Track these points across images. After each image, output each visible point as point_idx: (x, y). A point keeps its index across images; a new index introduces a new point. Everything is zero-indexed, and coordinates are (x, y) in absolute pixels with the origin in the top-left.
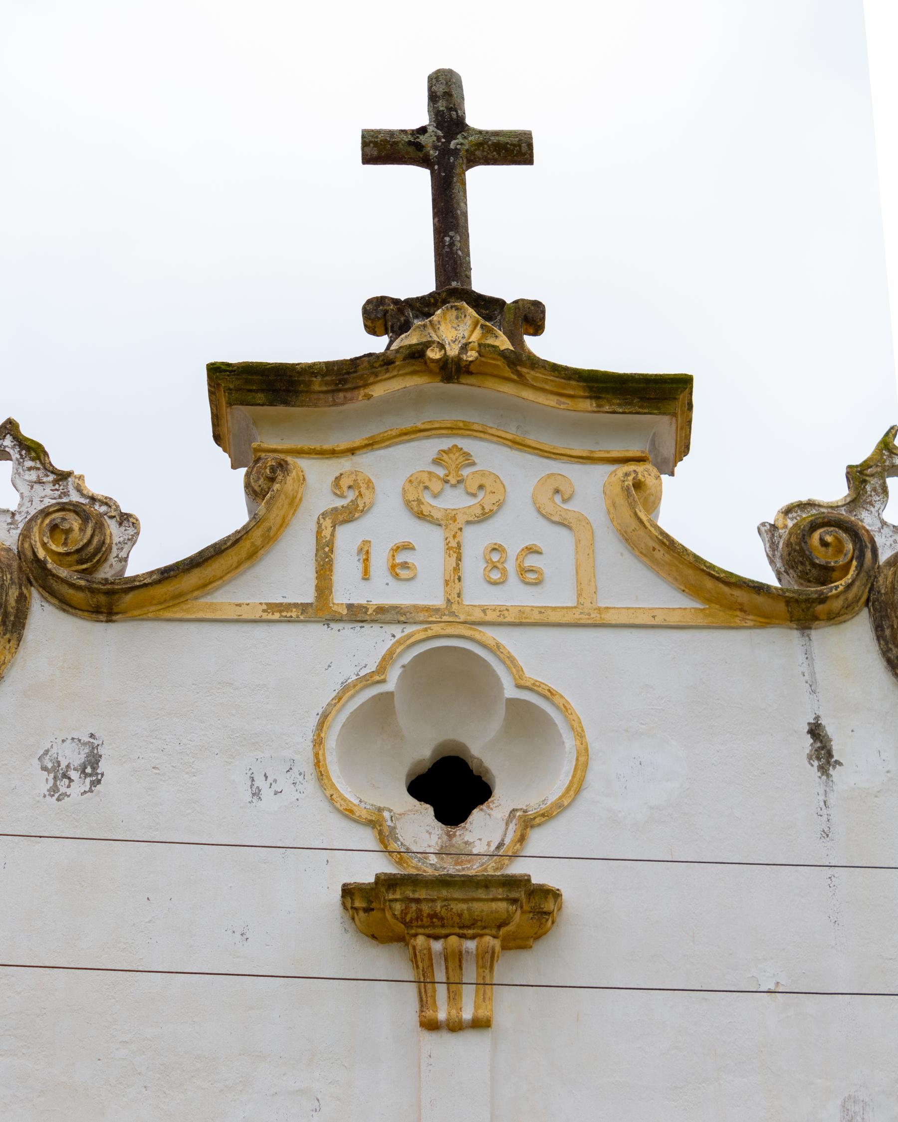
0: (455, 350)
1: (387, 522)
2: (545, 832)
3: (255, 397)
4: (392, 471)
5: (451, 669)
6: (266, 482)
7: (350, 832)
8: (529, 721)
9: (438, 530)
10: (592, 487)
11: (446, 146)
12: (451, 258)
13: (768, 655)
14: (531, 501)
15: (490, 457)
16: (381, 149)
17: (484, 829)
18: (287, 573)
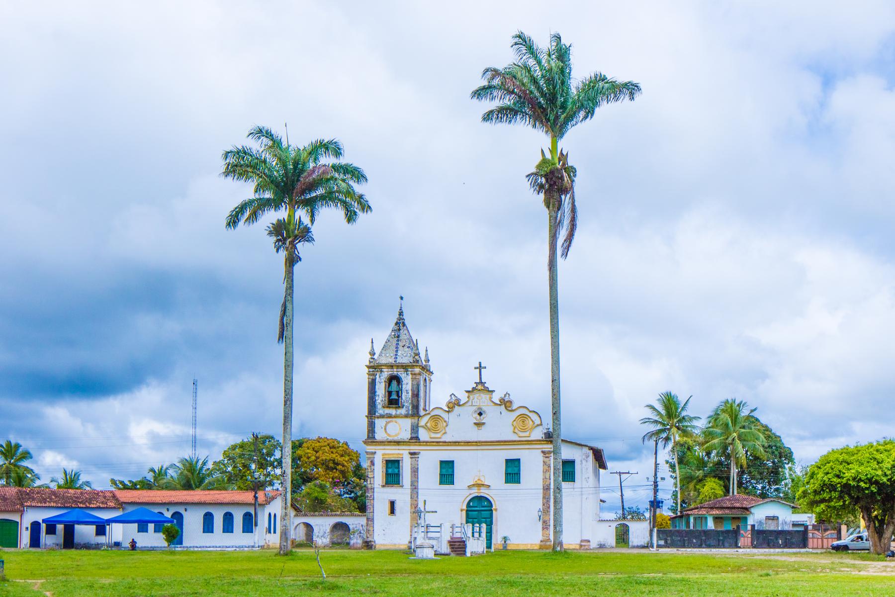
0: (480, 387)
1: (476, 400)
3: (468, 392)
4: (476, 396)
5: (480, 408)
10: (488, 396)
11: (480, 367)
14: (485, 397)
16: (476, 368)
18: (470, 403)
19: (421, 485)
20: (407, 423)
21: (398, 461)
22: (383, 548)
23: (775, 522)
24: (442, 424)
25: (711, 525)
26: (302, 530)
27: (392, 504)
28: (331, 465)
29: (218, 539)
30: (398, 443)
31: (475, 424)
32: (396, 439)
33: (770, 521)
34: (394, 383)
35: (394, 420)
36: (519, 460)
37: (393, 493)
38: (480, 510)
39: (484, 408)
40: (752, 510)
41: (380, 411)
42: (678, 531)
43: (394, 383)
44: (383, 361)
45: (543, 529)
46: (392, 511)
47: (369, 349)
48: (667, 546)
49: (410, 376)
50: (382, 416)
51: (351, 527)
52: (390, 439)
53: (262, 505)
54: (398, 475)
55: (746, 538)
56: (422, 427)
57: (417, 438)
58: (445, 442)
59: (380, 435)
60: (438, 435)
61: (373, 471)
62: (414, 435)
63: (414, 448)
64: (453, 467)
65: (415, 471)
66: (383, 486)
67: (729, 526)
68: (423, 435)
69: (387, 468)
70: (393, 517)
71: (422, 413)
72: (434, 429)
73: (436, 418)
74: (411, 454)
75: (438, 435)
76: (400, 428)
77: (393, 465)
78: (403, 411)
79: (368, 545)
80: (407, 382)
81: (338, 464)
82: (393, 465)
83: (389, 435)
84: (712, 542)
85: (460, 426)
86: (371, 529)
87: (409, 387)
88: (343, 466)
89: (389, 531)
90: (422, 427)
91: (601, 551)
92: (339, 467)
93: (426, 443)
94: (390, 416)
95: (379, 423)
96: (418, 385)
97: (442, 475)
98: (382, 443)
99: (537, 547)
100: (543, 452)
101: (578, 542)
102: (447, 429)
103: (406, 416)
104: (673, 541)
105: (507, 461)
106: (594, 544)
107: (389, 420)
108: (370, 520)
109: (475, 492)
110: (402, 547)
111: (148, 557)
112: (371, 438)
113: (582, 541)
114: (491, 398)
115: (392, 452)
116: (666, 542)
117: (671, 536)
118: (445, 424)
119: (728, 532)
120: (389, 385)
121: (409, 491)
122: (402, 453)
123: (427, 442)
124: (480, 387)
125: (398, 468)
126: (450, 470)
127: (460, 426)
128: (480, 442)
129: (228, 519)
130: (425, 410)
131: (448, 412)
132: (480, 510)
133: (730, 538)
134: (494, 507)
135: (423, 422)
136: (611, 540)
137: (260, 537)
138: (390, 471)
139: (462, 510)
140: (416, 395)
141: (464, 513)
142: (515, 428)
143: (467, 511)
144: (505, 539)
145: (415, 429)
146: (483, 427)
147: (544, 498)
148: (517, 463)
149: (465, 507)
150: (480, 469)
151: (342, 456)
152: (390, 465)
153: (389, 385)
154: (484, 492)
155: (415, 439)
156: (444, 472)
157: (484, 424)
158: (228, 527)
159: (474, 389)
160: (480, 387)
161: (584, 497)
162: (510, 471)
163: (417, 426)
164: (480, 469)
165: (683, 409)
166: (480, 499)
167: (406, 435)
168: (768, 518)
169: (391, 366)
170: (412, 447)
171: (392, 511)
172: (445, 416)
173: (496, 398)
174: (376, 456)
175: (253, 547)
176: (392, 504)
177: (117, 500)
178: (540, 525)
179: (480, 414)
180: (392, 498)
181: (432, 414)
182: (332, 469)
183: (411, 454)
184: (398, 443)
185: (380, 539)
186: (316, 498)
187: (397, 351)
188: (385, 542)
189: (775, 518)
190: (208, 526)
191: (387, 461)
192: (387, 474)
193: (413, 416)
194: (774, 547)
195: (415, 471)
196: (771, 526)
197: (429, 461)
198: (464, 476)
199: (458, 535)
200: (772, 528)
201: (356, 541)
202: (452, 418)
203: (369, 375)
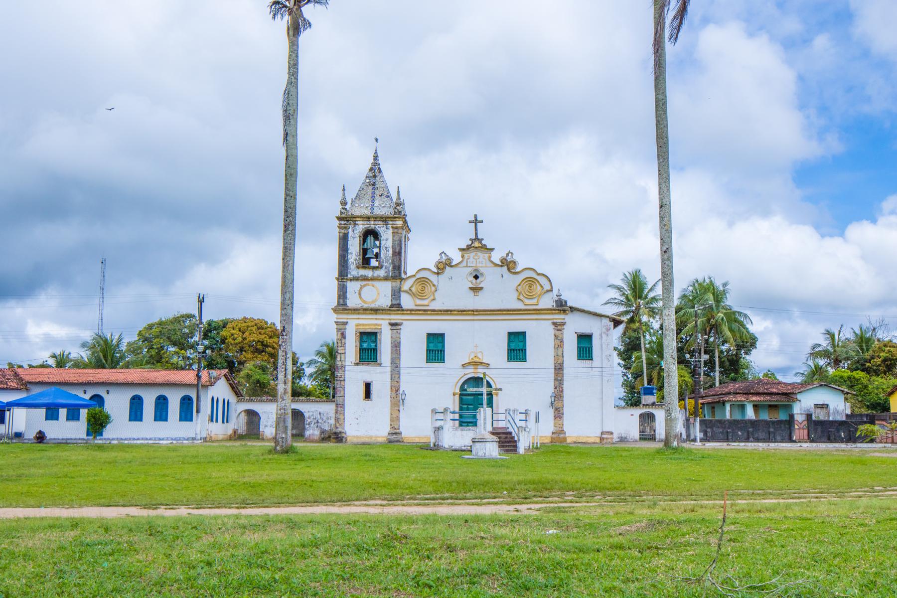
0: (476, 245)
1: (471, 259)
2: (483, 283)
3: (462, 250)
4: (472, 255)
6: (463, 257)
7: (470, 282)
8: (482, 274)
9: (477, 260)
10: (487, 256)
12: (476, 234)
13: (500, 268)
14: (482, 256)
15: (479, 254)
17: (478, 281)
18: (464, 264)
19: (404, 361)
20: (386, 288)
21: (375, 334)
22: (355, 440)
23: (825, 411)
24: (429, 289)
25: (750, 413)
26: (243, 418)
27: (368, 386)
28: (260, 347)
29: (148, 429)
30: (376, 311)
31: (471, 288)
32: (373, 306)
33: (819, 410)
34: (370, 238)
35: (370, 282)
36: (523, 334)
37: (368, 373)
39: (482, 270)
40: (799, 397)
41: (353, 272)
42: (720, 421)
43: (370, 238)
44: (357, 211)
45: (555, 417)
46: (368, 395)
47: (340, 198)
48: (705, 439)
49: (391, 230)
50: (356, 279)
51: (306, 415)
52: (366, 306)
53: (205, 387)
54: (375, 350)
55: (799, 432)
56: (406, 292)
57: (399, 305)
58: (434, 311)
59: (353, 301)
60: (425, 302)
61: (344, 345)
62: (395, 302)
63: (396, 318)
64: (443, 342)
66: (357, 364)
67: (765, 416)
68: (407, 301)
69: (361, 341)
70: (368, 403)
71: (403, 276)
72: (420, 295)
73: (423, 281)
74: (392, 324)
75: (425, 302)
76: (379, 293)
77: (368, 338)
78: (381, 273)
79: (337, 437)
80: (387, 236)
81: (267, 346)
82: (368, 338)
83: (365, 302)
84: (761, 435)
85: (452, 291)
86: (341, 417)
87: (390, 243)
88: (274, 348)
89: (364, 421)
90: (406, 292)
91: (623, 445)
92: (269, 350)
93: (411, 311)
94: (365, 278)
95: (352, 287)
96: (400, 241)
98: (355, 311)
99: (547, 441)
100: (554, 324)
101: (599, 435)
102: (436, 294)
103: (386, 279)
104: (713, 432)
105: (510, 334)
106: (615, 437)
107: (364, 283)
108: (340, 407)
109: (471, 372)
110: (380, 440)
111: (64, 454)
112: (342, 306)
113: (602, 433)
114: (490, 257)
115: (368, 322)
116: (705, 433)
117: (711, 427)
118: (433, 288)
119: (780, 422)
120: (364, 241)
121: (389, 370)
122: (381, 324)
123: (411, 310)
124: (477, 244)
125: (375, 341)
126: (440, 345)
127: (452, 291)
128: (477, 311)
129: (162, 403)
130: (405, 273)
131: (438, 274)
133: (783, 430)
135: (406, 286)
136: (635, 433)
137: (201, 426)
138: (365, 345)
139: (454, 394)
140: (398, 253)
141: (457, 397)
142: (520, 293)
143: (460, 395)
145: (396, 293)
146: (481, 293)
147: (555, 379)
148: (521, 337)
149: (458, 391)
150: (477, 344)
151: (271, 337)
152: (365, 338)
153: (364, 241)
155: (396, 307)
156: (432, 347)
157: (481, 288)
158: (161, 412)
159: (469, 247)
160: (476, 245)
161: (605, 379)
162: (513, 346)
163: (400, 291)
164: (477, 344)
165: (651, 289)
166: (477, 381)
167: (385, 301)
168: (817, 406)
169: (368, 218)
170: (393, 317)
171: (368, 395)
172: (433, 278)
173: (496, 257)
174: (347, 327)
175: (194, 439)
176: (368, 386)
177: (21, 379)
178: (551, 412)
179: (476, 277)
180: (368, 380)
181: (418, 277)
182: (260, 352)
183: (392, 324)
184: (376, 311)
185: (353, 430)
186: (258, 381)
187: (373, 201)
188: (359, 434)
189: (824, 407)
190: (136, 413)
191: (362, 334)
192: (362, 350)
193: (394, 278)
194: (835, 441)
195: (396, 346)
196: (820, 415)
197: (414, 333)
198: (457, 352)
199: (502, 424)
200: (822, 418)
201: (312, 432)
202: (442, 282)
203: (340, 228)
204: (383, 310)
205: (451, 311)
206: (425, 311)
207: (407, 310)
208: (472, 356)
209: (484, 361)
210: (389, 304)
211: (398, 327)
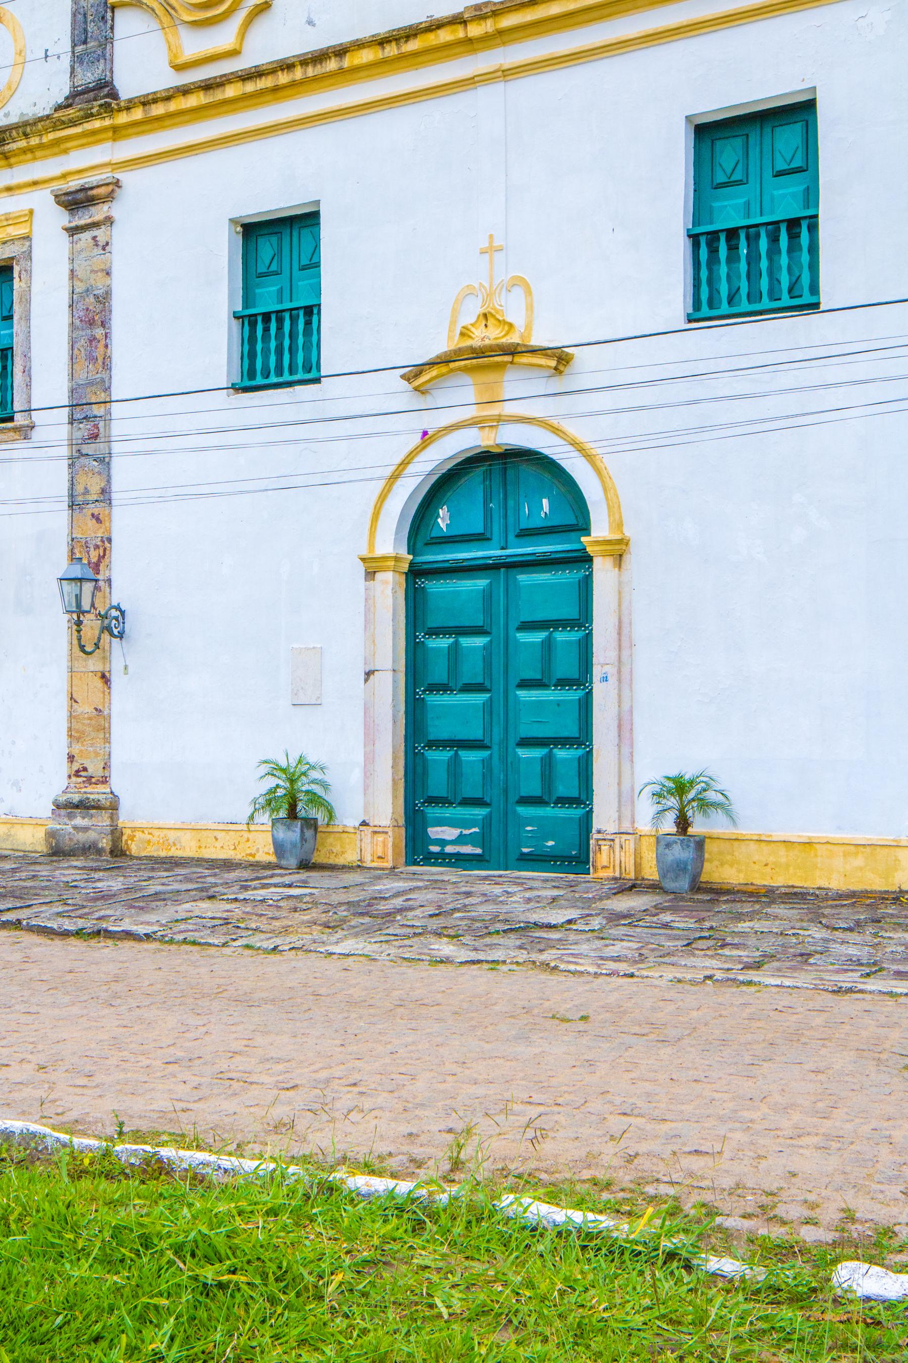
38: (497, 565)
58: (256, 74)
62: (88, 77)
63: (85, 161)
65: (92, 318)
97: (253, 324)
132: (497, 565)
134: (600, 528)
139: (372, 568)
141: (389, 590)
143: (416, 574)
144: (685, 796)
149: (390, 542)
154: (525, 412)
166: (502, 468)
195: (92, 318)
204: (25, 128)
205: (341, 52)
206: (208, 86)
207: (130, 106)
208: (468, 317)
209: (536, 341)
210: (66, 92)
211: (98, 213)
